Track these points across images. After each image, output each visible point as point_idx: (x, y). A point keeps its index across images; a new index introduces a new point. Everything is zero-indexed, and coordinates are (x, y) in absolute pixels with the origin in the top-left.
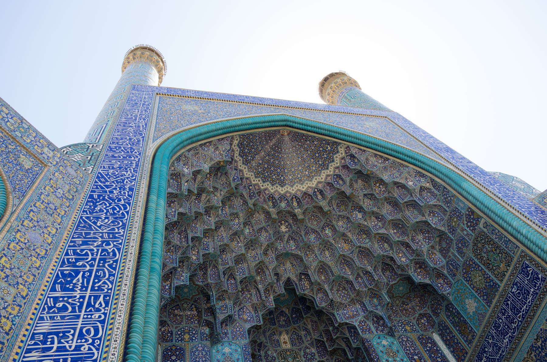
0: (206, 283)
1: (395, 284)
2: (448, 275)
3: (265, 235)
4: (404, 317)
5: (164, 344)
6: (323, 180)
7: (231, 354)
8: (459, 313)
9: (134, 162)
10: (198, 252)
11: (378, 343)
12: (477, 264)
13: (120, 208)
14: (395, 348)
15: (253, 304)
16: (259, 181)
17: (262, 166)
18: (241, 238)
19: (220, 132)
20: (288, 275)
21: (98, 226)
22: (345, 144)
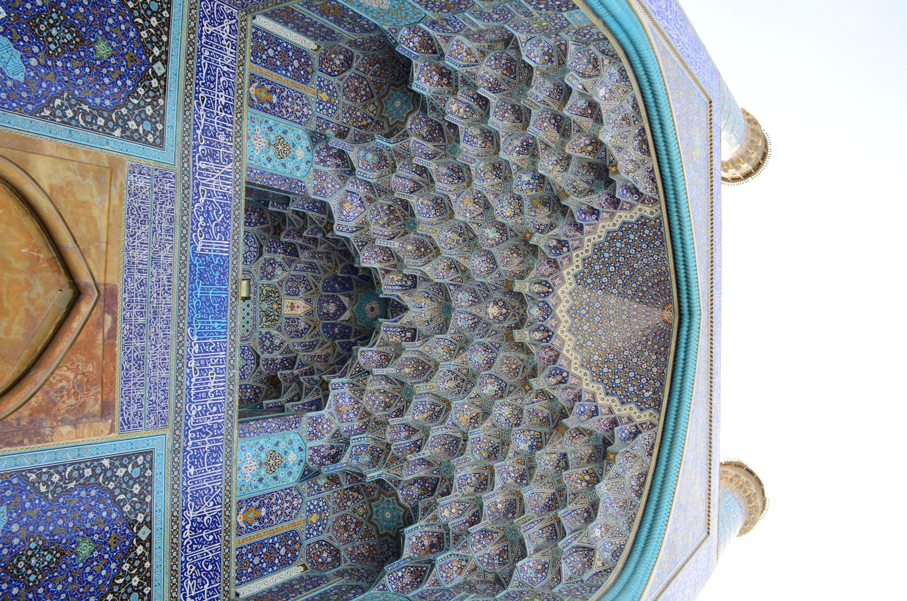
0: (409, 132)
1: (398, 499)
2: (420, 590)
3: (482, 269)
4: (333, 517)
5: (315, 57)
6: (585, 387)
7: (293, 158)
10: (462, 118)
14: (281, 473)
15: (369, 224)
16: (577, 266)
17: (604, 271)
18: (479, 218)
19: (667, 170)
20: (412, 309)
22: (659, 420)
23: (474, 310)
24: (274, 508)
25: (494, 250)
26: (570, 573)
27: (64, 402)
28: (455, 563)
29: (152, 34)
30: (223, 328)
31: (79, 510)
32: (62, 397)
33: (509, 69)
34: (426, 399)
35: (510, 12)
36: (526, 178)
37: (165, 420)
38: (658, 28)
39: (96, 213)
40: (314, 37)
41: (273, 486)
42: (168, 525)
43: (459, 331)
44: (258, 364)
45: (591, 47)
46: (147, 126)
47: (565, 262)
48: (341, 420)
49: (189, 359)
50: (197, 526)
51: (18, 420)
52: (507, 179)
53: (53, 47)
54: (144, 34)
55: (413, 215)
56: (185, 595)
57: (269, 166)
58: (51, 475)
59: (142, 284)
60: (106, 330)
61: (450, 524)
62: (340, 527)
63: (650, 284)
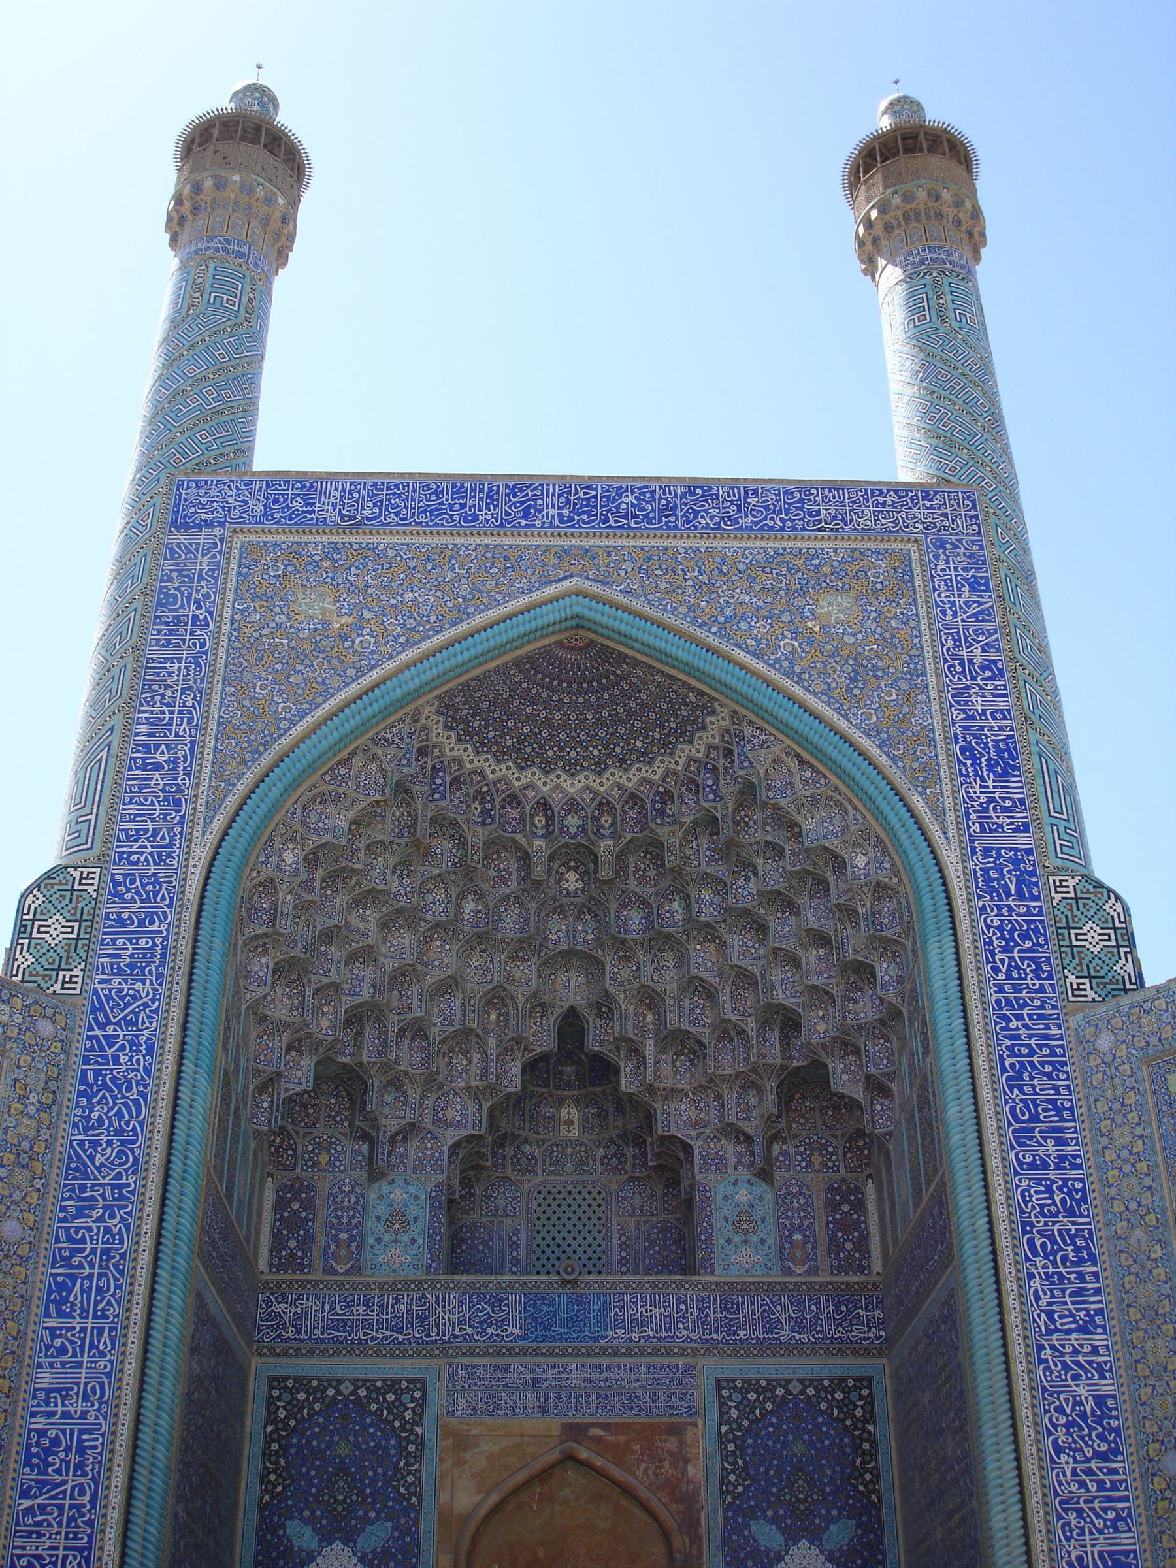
0: (357, 1060)
3: (517, 911)
7: (406, 1205)
9: (158, 941)
11: (726, 1198)
13: (131, 1115)
14: (758, 1213)
21: (96, 1167)
28: (876, 1041)
29: (315, 1397)
30: (599, 1299)
36: (394, 884)
39: (497, 1449)
41: (770, 1221)
42: (794, 1361)
46: (406, 1398)
49: (631, 1340)
50: (799, 1325)
51: (679, 1513)
52: (400, 911)
53: (354, 1498)
54: (317, 1406)
56: (865, 1339)
57: (421, 1241)
58: (730, 1482)
59: (558, 1398)
60: (602, 1433)
63: (532, 672)
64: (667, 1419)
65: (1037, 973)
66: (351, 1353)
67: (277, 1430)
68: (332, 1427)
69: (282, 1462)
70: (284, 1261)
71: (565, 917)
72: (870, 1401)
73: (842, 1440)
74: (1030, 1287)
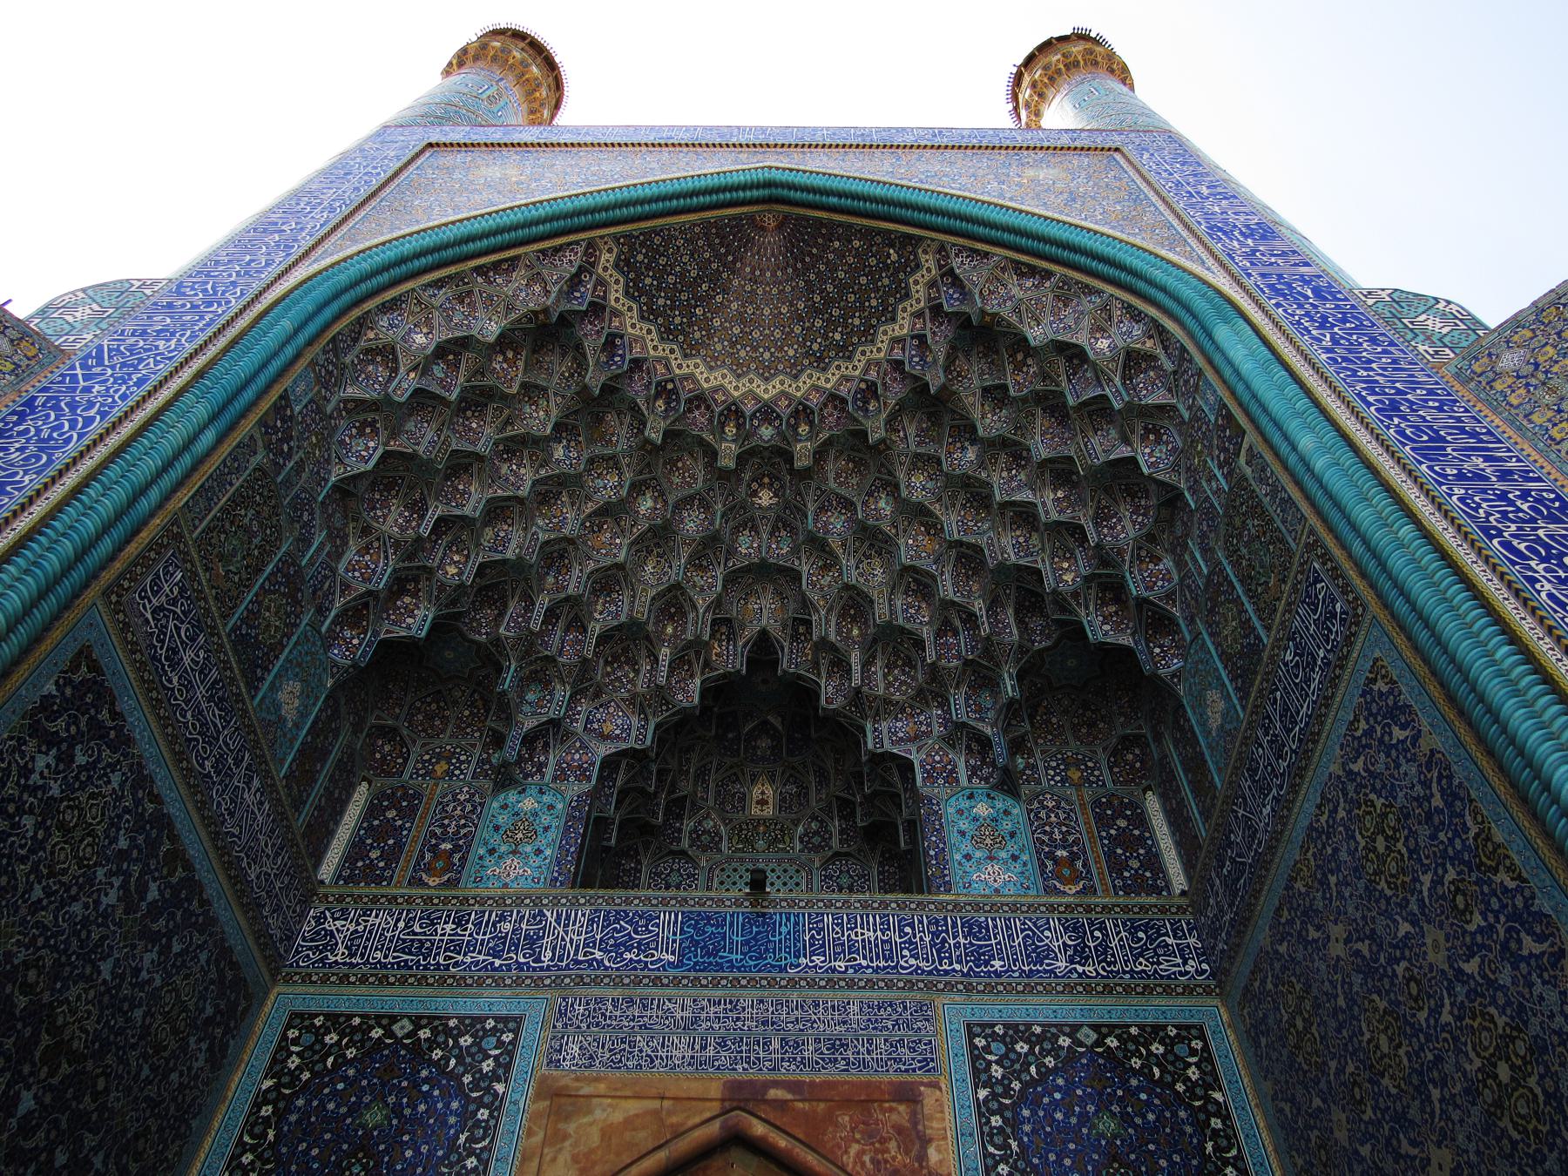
1: (1047, 649)
4: (1073, 748)
7: (536, 814)
8: (1193, 733)
10: (468, 557)
11: (960, 812)
12: (1230, 583)
14: (1007, 825)
20: (764, 622)
22: (933, 240)
23: (765, 531)
24: (1058, 836)
25: (672, 499)
26: (1162, 391)
27: (894, 1158)
30: (788, 919)
31: (1050, 1134)
32: (886, 1161)
33: (389, 488)
34: (899, 603)
35: (297, 496)
37: (921, 1006)
38: (313, 248)
39: (618, 1117)
40: (349, 789)
41: (1025, 838)
43: (795, 551)
44: (847, 854)
45: (348, 360)
47: (689, 386)
48: (928, 734)
49: (834, 970)
54: (351, 1053)
55: (619, 627)
57: (548, 852)
61: (1084, 573)
62: (1089, 734)
63: (723, 250)
64: (894, 1078)
65: (1373, 341)
66: (422, 981)
67: (277, 1087)
68: (364, 1083)
69: (271, 1134)
70: (357, 866)
71: (757, 533)
72: (1206, 1057)
73: (1175, 1114)
74: (1539, 592)
